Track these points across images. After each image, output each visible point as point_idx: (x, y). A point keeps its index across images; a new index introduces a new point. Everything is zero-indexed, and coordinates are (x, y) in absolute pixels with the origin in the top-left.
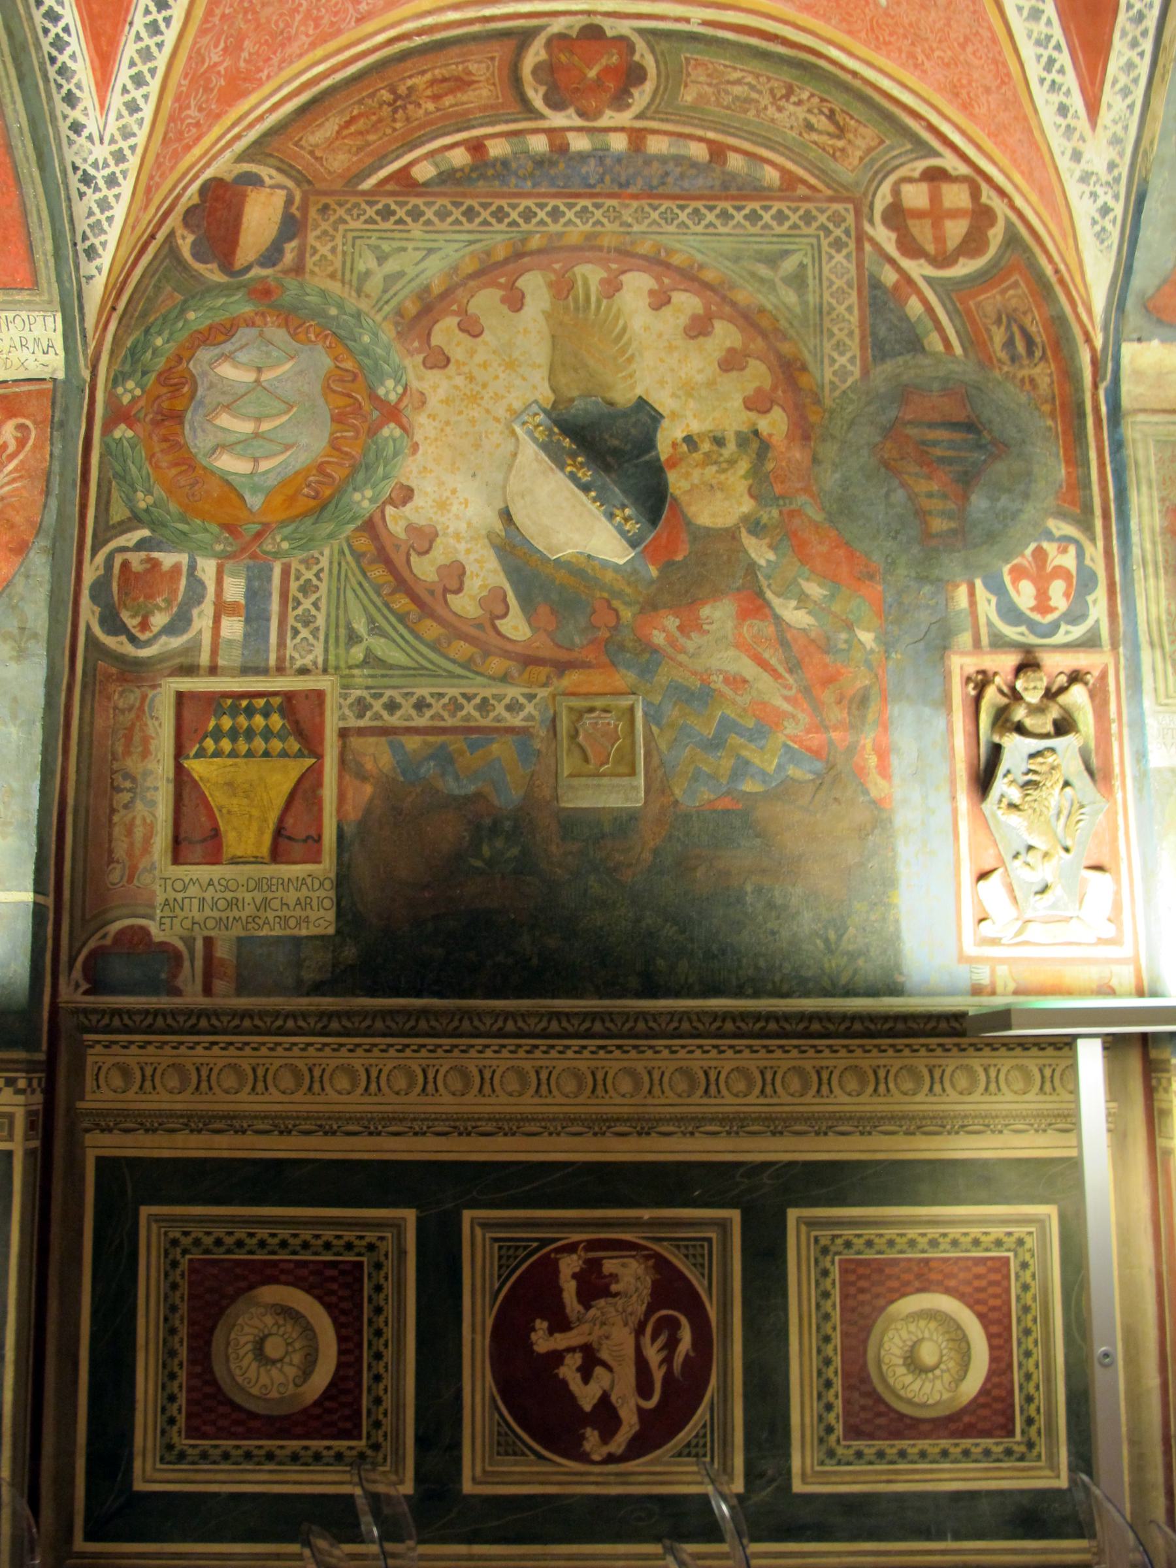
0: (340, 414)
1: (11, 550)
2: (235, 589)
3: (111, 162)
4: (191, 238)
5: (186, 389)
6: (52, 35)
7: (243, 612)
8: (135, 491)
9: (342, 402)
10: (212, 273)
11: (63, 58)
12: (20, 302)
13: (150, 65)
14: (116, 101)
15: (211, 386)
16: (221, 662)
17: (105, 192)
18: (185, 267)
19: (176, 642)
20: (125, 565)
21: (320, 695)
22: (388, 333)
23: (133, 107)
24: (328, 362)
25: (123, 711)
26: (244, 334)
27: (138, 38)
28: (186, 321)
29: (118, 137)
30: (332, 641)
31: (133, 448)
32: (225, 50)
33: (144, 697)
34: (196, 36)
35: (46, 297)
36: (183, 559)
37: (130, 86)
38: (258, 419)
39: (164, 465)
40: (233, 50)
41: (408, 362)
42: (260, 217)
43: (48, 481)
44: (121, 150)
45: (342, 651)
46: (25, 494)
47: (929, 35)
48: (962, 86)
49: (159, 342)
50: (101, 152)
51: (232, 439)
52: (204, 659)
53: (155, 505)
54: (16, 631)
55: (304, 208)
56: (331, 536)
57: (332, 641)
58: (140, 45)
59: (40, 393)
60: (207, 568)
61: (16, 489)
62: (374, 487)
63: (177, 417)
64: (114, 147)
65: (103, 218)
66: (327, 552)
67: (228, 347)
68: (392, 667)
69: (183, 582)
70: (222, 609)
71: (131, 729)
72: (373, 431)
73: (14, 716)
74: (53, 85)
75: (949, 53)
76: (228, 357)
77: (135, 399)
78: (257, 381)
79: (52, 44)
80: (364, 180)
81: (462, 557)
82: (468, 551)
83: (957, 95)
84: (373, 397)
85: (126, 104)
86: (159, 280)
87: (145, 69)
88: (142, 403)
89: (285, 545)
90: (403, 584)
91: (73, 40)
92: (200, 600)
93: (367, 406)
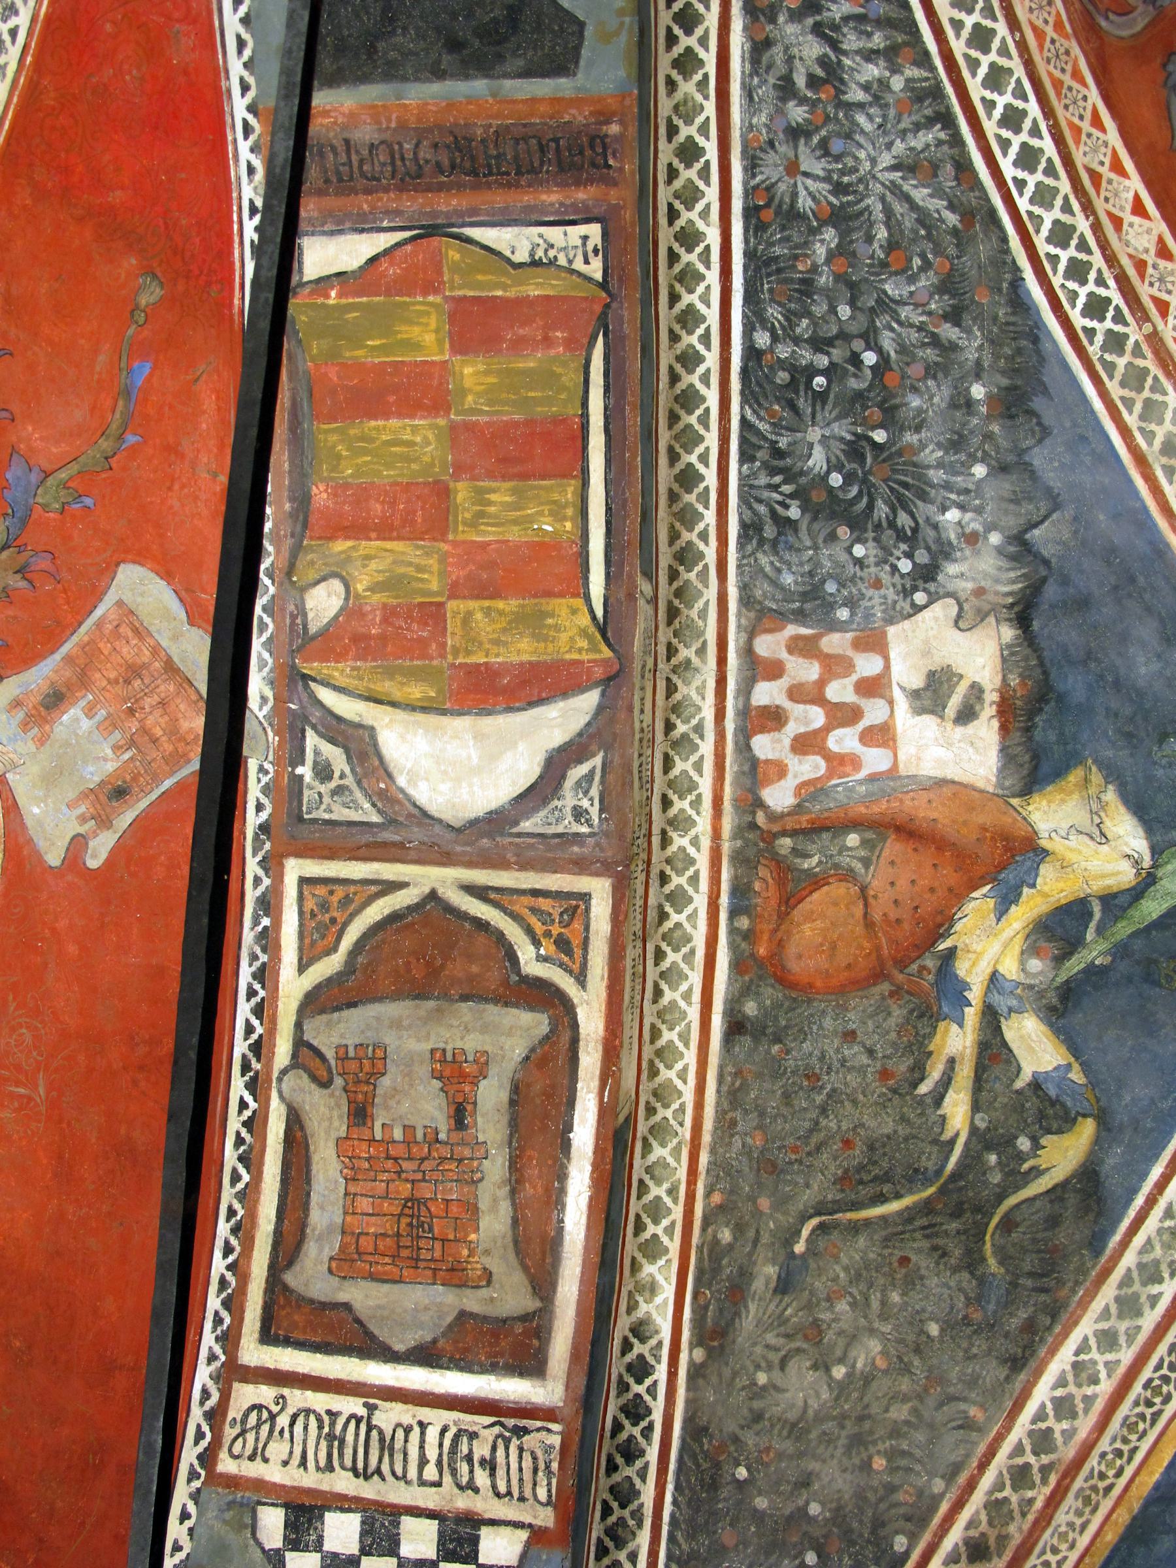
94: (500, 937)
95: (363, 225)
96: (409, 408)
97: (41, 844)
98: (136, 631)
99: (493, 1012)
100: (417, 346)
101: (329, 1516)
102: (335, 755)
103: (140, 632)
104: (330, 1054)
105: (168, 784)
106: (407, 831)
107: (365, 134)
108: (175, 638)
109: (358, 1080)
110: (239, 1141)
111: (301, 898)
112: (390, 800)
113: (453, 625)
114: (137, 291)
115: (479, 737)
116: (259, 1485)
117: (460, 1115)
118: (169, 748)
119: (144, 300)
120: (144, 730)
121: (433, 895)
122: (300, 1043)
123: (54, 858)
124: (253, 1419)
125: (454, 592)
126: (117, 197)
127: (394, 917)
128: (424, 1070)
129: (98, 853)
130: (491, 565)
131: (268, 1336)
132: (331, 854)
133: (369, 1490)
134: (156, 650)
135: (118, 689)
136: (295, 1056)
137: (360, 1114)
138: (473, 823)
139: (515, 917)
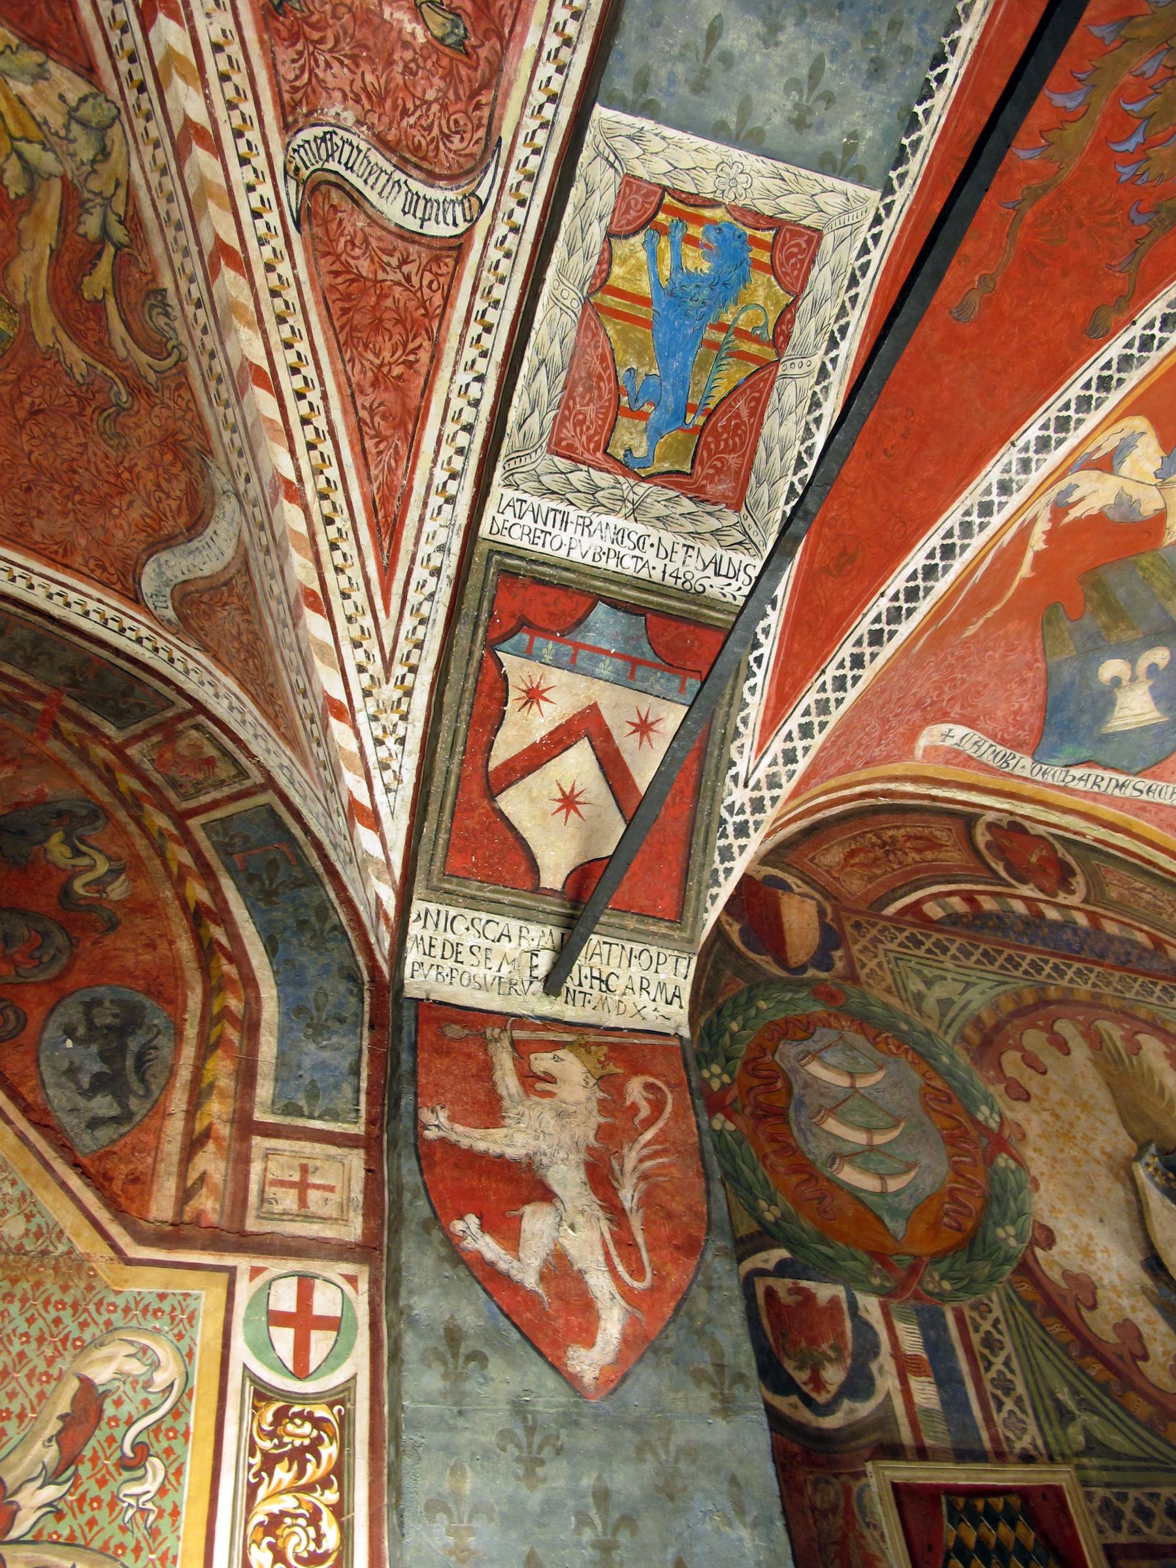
0: (951, 1136)
1: (677, 1248)
2: (911, 1340)
3: (748, 809)
4: (736, 927)
5: (779, 1084)
7: (929, 1370)
8: (756, 1198)
9: (947, 1123)
10: (766, 963)
12: (654, 934)
13: (823, 718)
14: (777, 746)
15: (806, 1085)
16: (928, 1442)
17: (731, 840)
18: (740, 955)
19: (865, 1409)
20: (770, 1293)
21: (1056, 1493)
22: (964, 1059)
23: (790, 757)
24: (916, 1077)
25: (825, 1514)
26: (823, 1036)
27: (823, 688)
28: (758, 1009)
29: (763, 784)
30: (1042, 1417)
31: (740, 1144)
33: (848, 1491)
35: (686, 935)
36: (840, 1291)
38: (869, 1130)
39: (782, 1170)
41: (991, 1089)
42: (800, 918)
43: (702, 1159)
44: (762, 798)
45: (1059, 1432)
46: (675, 1172)
49: (734, 1026)
50: (740, 796)
51: (848, 1149)
52: (906, 1435)
53: (783, 1218)
54: (710, 1369)
55: (837, 918)
56: (992, 1278)
57: (1042, 1417)
59: (666, 1048)
60: (870, 1306)
61: (663, 1166)
62: (1013, 1223)
63: (781, 1115)
64: (756, 794)
65: (721, 868)
66: (994, 1297)
67: (811, 1045)
68: (1119, 1456)
69: (848, 1324)
70: (905, 1366)
71: (843, 1543)
72: (990, 1161)
73: (740, 1511)
76: (816, 1055)
77: (724, 1087)
78: (852, 1087)
80: (887, 904)
81: (1131, 1316)
82: (1133, 1308)
84: (975, 1122)
85: (785, 752)
86: (716, 962)
87: (816, 721)
88: (734, 1092)
89: (946, 1285)
90: (1089, 1346)
92: (875, 1351)
93: (974, 1133)
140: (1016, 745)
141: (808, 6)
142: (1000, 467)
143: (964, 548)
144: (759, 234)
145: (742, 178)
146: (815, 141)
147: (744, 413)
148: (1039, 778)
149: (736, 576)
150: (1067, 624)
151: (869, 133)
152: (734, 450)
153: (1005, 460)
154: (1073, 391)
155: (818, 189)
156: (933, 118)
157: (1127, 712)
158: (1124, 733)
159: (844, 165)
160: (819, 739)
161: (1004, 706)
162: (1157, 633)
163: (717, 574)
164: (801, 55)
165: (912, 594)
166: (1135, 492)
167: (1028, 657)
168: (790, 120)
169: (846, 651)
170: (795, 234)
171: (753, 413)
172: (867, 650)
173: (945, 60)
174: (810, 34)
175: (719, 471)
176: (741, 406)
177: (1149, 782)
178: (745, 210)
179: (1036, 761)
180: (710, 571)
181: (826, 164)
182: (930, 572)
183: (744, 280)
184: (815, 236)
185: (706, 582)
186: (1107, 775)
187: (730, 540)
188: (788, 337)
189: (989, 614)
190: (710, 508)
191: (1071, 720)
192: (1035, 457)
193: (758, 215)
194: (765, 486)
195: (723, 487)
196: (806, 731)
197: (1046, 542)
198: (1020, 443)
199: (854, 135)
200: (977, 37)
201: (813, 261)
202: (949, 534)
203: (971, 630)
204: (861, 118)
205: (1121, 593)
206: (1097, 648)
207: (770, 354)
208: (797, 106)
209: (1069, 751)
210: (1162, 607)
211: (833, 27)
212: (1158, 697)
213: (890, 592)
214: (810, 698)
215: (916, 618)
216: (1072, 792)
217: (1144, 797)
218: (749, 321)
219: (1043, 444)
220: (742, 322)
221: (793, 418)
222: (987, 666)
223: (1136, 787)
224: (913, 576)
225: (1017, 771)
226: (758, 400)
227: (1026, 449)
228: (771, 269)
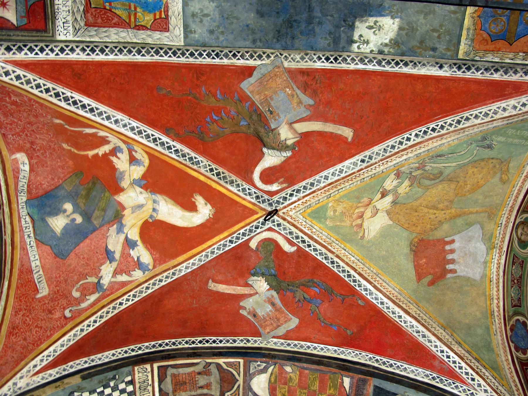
6: (35, 48)
11: (26, 50)
13: (25, 83)
14: (10, 68)
32: (16, 102)
34: (29, 97)
37: (16, 74)
40: (14, 103)
47: (33, 315)
48: (18, 330)
58: (32, 81)
74: (14, 43)
75: (31, 323)
79: (31, 47)
83: (14, 329)
91: (33, 55)
94: (231, 390)
95: (350, 387)
96: (320, 387)
97: (244, 301)
98: (286, 321)
99: (219, 390)
100: (330, 389)
101: (132, 386)
102: (262, 367)
103: (286, 322)
104: (209, 368)
105: (256, 324)
106: (248, 376)
107: (365, 392)
108: (284, 328)
109: (206, 372)
110: (190, 340)
111: (236, 362)
112: (254, 374)
113: (283, 386)
114: (350, 330)
115: (265, 388)
116: (134, 374)
117: (201, 387)
118: (263, 325)
119: (348, 331)
120: (267, 320)
121: (238, 380)
122: (210, 363)
123: (241, 304)
124: (144, 369)
125: (289, 387)
126: (368, 331)
127: (234, 375)
128: (208, 381)
129: (243, 312)
130: (293, 393)
131: (159, 367)
132: (244, 366)
133: (137, 389)
134: (282, 324)
135: (275, 317)
136: (208, 363)
137: (199, 373)
138: (250, 386)
139: (235, 392)
140: (29, 191)
141: (220, 8)
142: (122, 118)
143: (95, 115)
144: (163, 13)
145: (175, 3)
146: (190, 21)
147: (114, 21)
148: (20, 207)
149: (65, 29)
150: (77, 182)
151: (197, 36)
152: (103, 20)
153: (124, 119)
154: (150, 131)
155: (179, 26)
156: (204, 60)
157: (56, 221)
158: (48, 225)
159: (187, 32)
160: (17, 83)
161: (42, 178)
162: (86, 214)
163: (63, 23)
164: (209, 10)
165: (75, 103)
166: (127, 177)
167: (62, 176)
168: (193, 12)
169: (50, 85)
170: (166, 23)
171: (115, 24)
172: (52, 93)
173: (218, 58)
174: (214, 11)
175: (95, 16)
176: (116, 20)
177: (35, 245)
178: (168, 7)
179: (26, 202)
180: (64, 20)
181: (186, 27)
182: (84, 107)
183: (150, 12)
184: (167, 30)
185: (60, 20)
186: (31, 229)
187: (75, 25)
188: (139, 30)
189: (73, 150)
190: (83, 16)
191: (45, 204)
192: (128, 128)
193: (168, 11)
194: (95, 33)
195: (91, 19)
196: (18, 78)
197: (103, 155)
198: (131, 122)
199: (195, 32)
200: (225, 64)
201: (161, 31)
202: (97, 109)
203: (65, 146)
204: (200, 32)
205: (94, 193)
206: (73, 197)
207: (133, 25)
208: (197, 13)
209: (34, 212)
210: (95, 210)
211: (217, 16)
212: (65, 228)
213: (73, 95)
214: (30, 76)
215: (68, 107)
216: (20, 221)
217: (28, 247)
218: (139, 16)
219: (132, 129)
220: (139, 14)
221: (117, 37)
222: (54, 162)
223: (31, 241)
224: (81, 101)
225: (19, 198)
226: (119, 24)
227: (129, 124)
228: (155, 20)
